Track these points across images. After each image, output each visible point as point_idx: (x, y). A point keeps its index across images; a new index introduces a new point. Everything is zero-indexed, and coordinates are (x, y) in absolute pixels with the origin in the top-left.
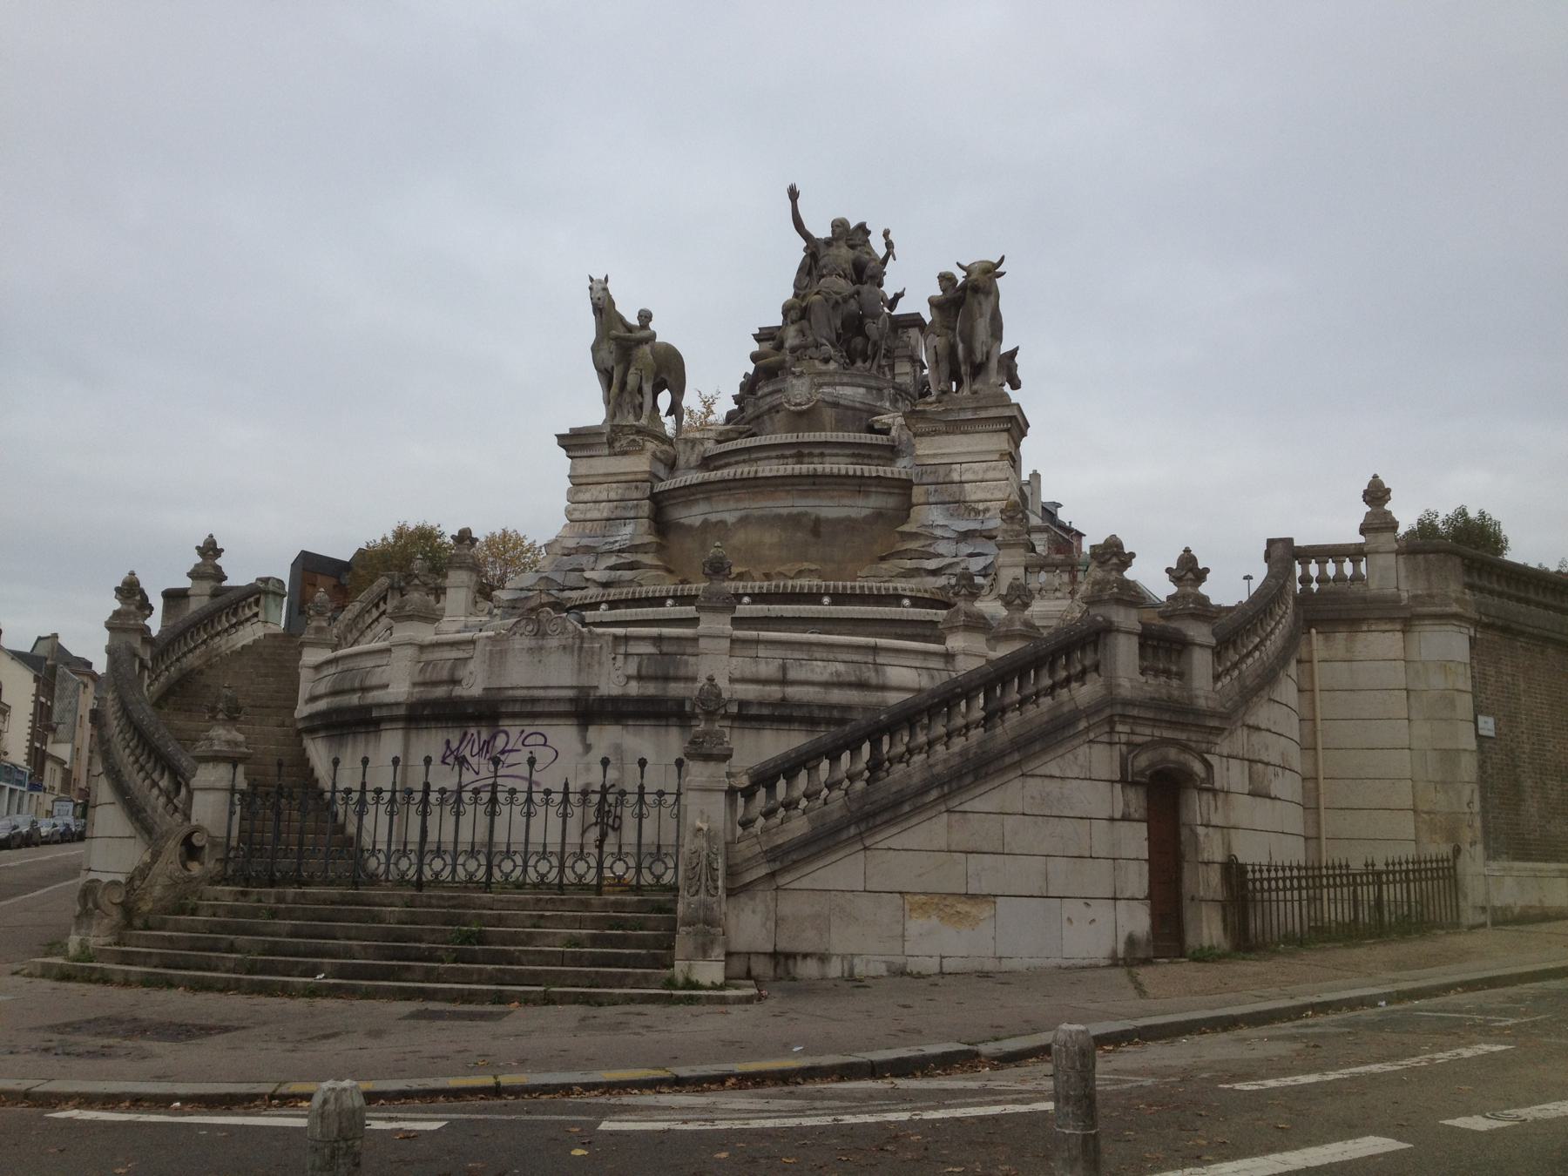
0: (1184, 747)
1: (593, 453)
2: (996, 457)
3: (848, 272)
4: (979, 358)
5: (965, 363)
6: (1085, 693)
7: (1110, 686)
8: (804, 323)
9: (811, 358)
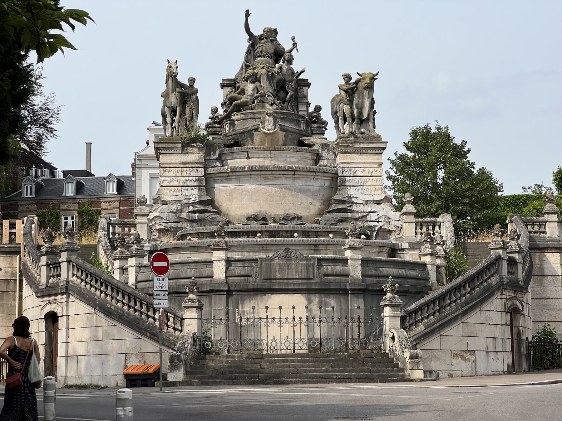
0: (517, 299)
1: (172, 152)
2: (377, 165)
3: (272, 55)
4: (365, 117)
6: (494, 281)
7: (501, 278)
8: (257, 83)
9: (263, 102)
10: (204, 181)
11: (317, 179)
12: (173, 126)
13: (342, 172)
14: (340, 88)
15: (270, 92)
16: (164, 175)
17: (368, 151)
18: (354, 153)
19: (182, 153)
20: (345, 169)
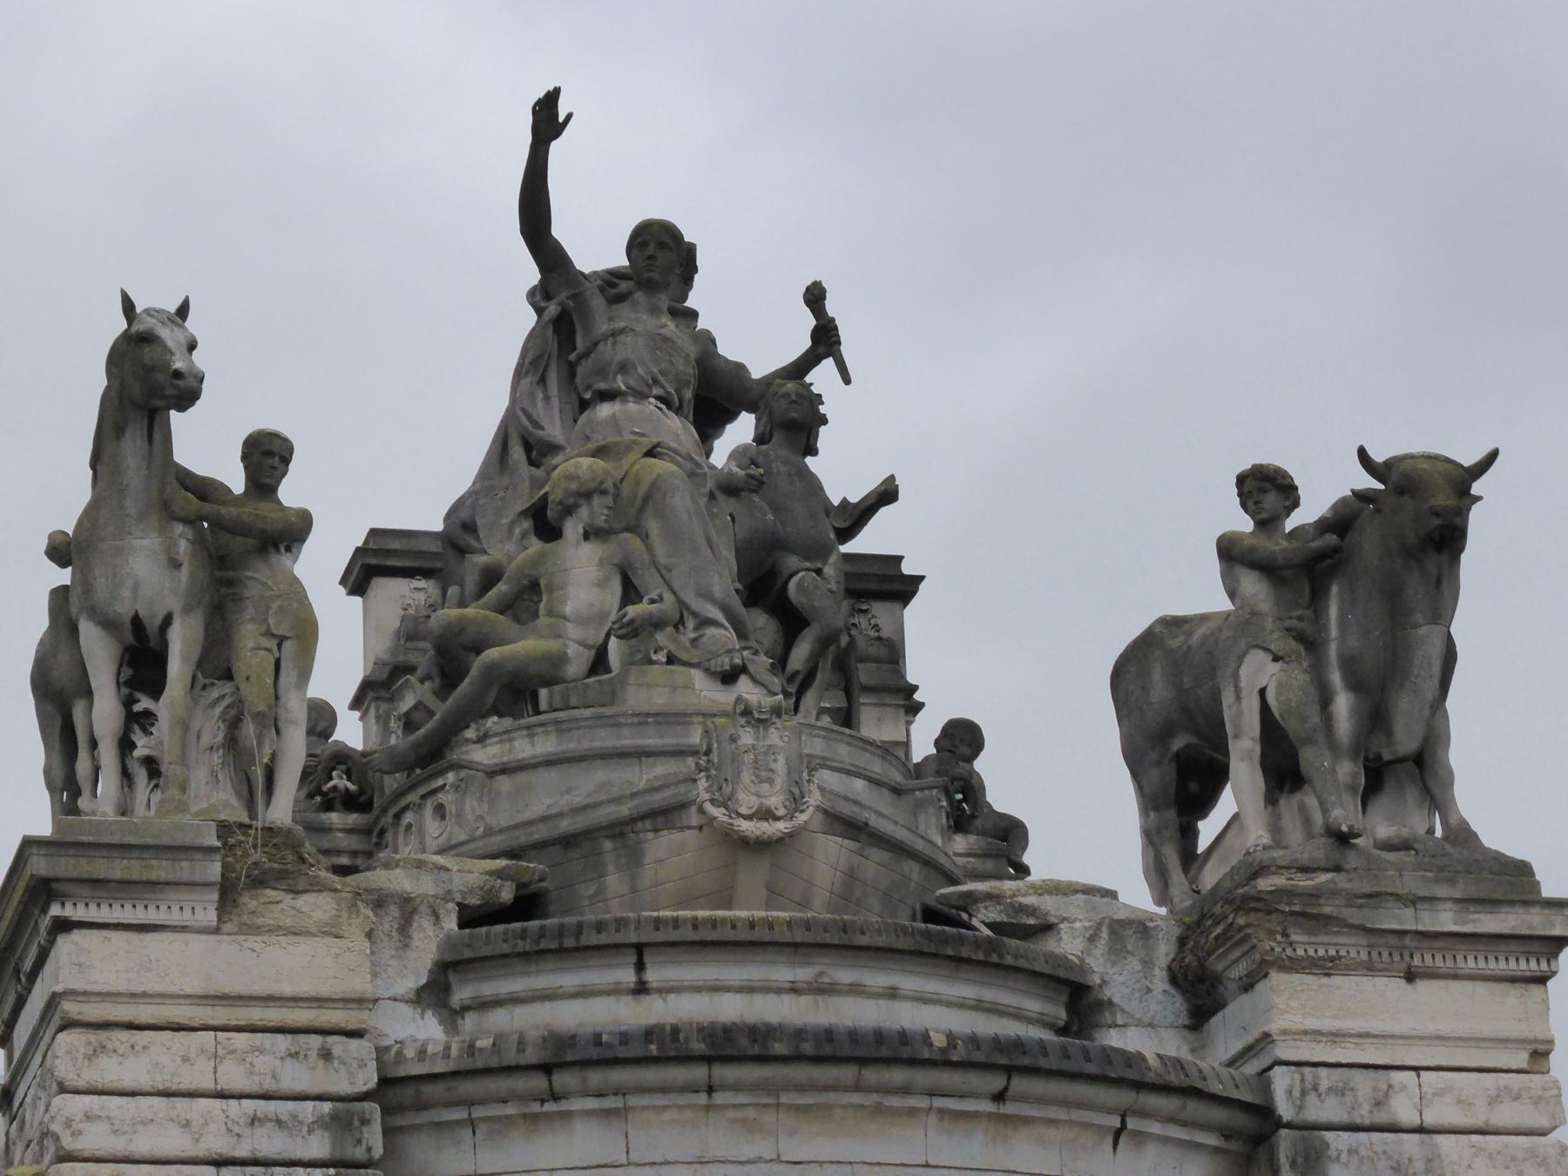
2: (1521, 1059)
5: (1354, 758)
9: (671, 660)
10: (377, 1126)
11: (1140, 1137)
12: (137, 753)
13: (1296, 1093)
14: (1230, 552)
15: (713, 601)
16: (90, 1076)
17: (1460, 958)
18: (1370, 969)
19: (216, 931)
20: (1316, 1078)
